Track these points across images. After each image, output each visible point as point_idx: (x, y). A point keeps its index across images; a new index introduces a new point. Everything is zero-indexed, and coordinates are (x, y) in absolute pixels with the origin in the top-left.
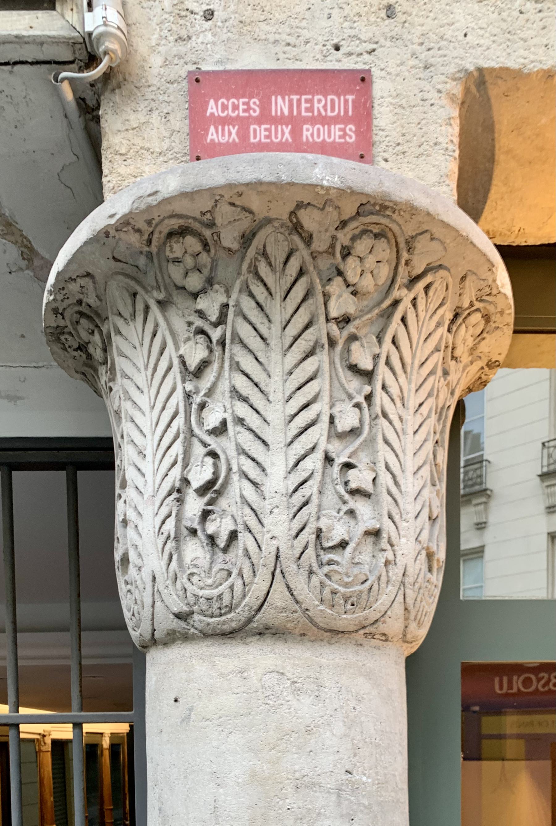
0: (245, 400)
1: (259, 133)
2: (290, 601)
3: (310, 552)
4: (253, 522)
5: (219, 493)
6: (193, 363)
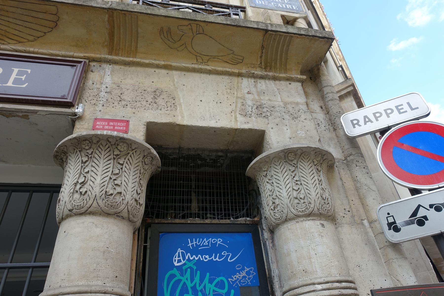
0: (94, 167)
1: (107, 127)
2: (97, 205)
3: (104, 195)
4: (91, 189)
5: (85, 184)
6: (84, 161)
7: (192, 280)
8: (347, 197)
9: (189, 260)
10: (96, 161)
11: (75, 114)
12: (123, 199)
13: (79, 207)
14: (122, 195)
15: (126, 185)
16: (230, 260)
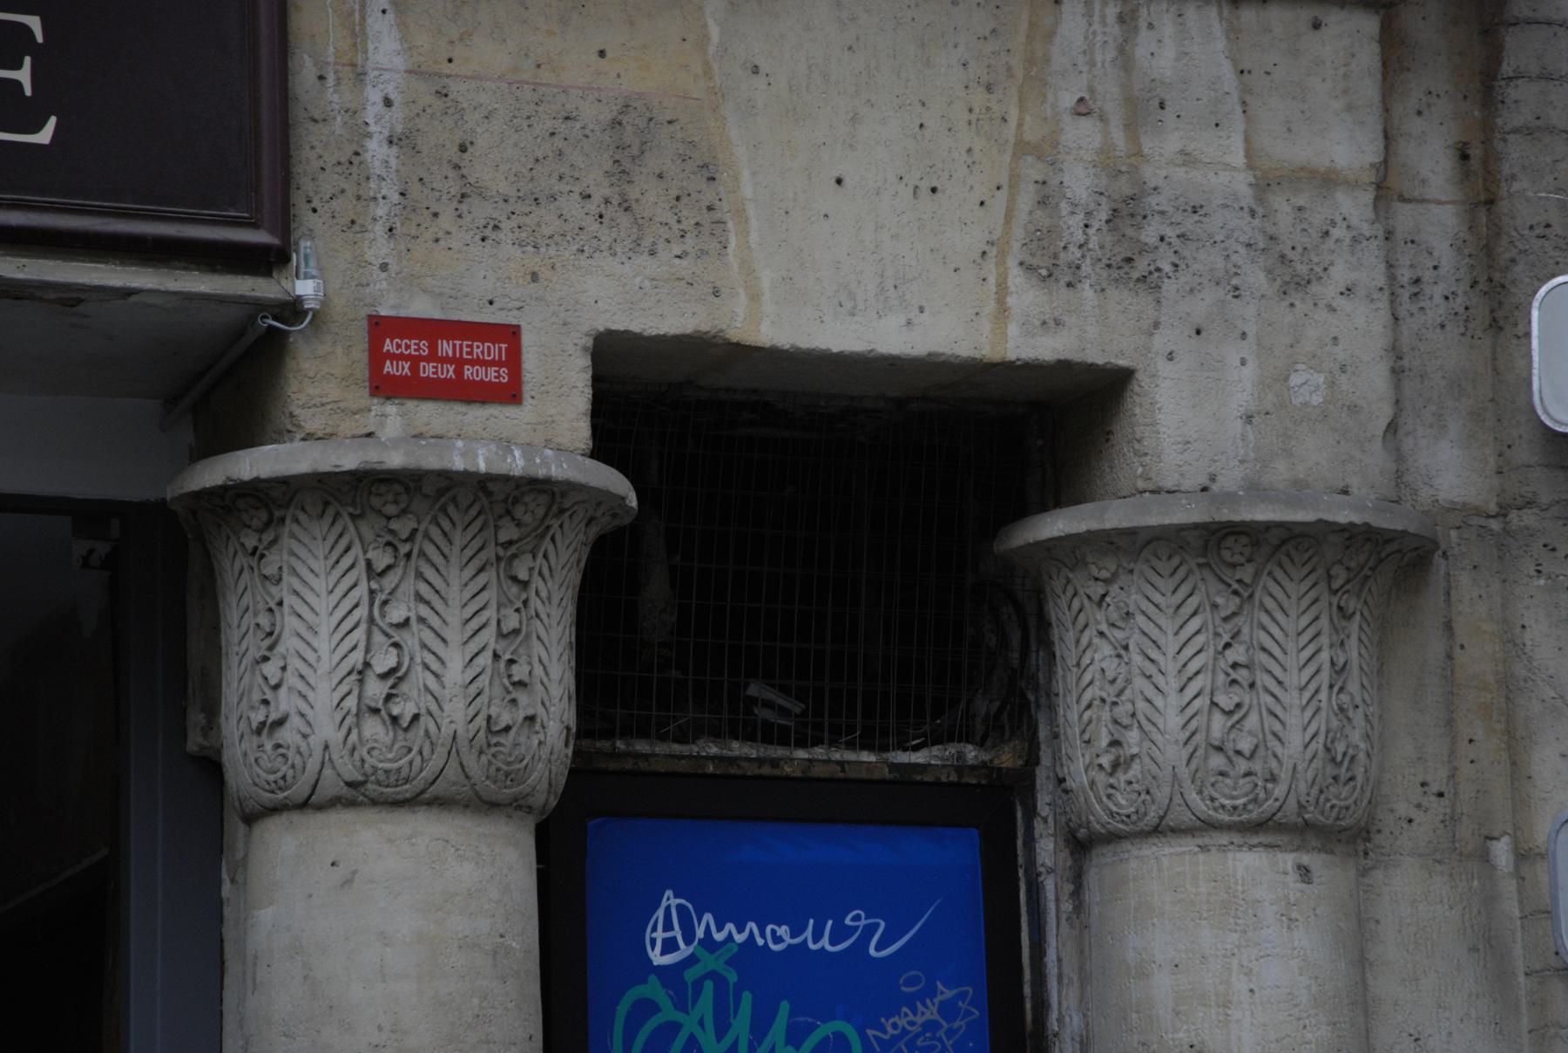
0: (428, 603)
2: (462, 776)
3: (482, 734)
4: (434, 707)
6: (380, 565)
7: (722, 1029)
8: (1450, 723)
9: (708, 943)
10: (430, 573)
11: (292, 310)
12: (540, 743)
13: (392, 779)
14: (538, 727)
15: (545, 680)
16: (878, 949)
